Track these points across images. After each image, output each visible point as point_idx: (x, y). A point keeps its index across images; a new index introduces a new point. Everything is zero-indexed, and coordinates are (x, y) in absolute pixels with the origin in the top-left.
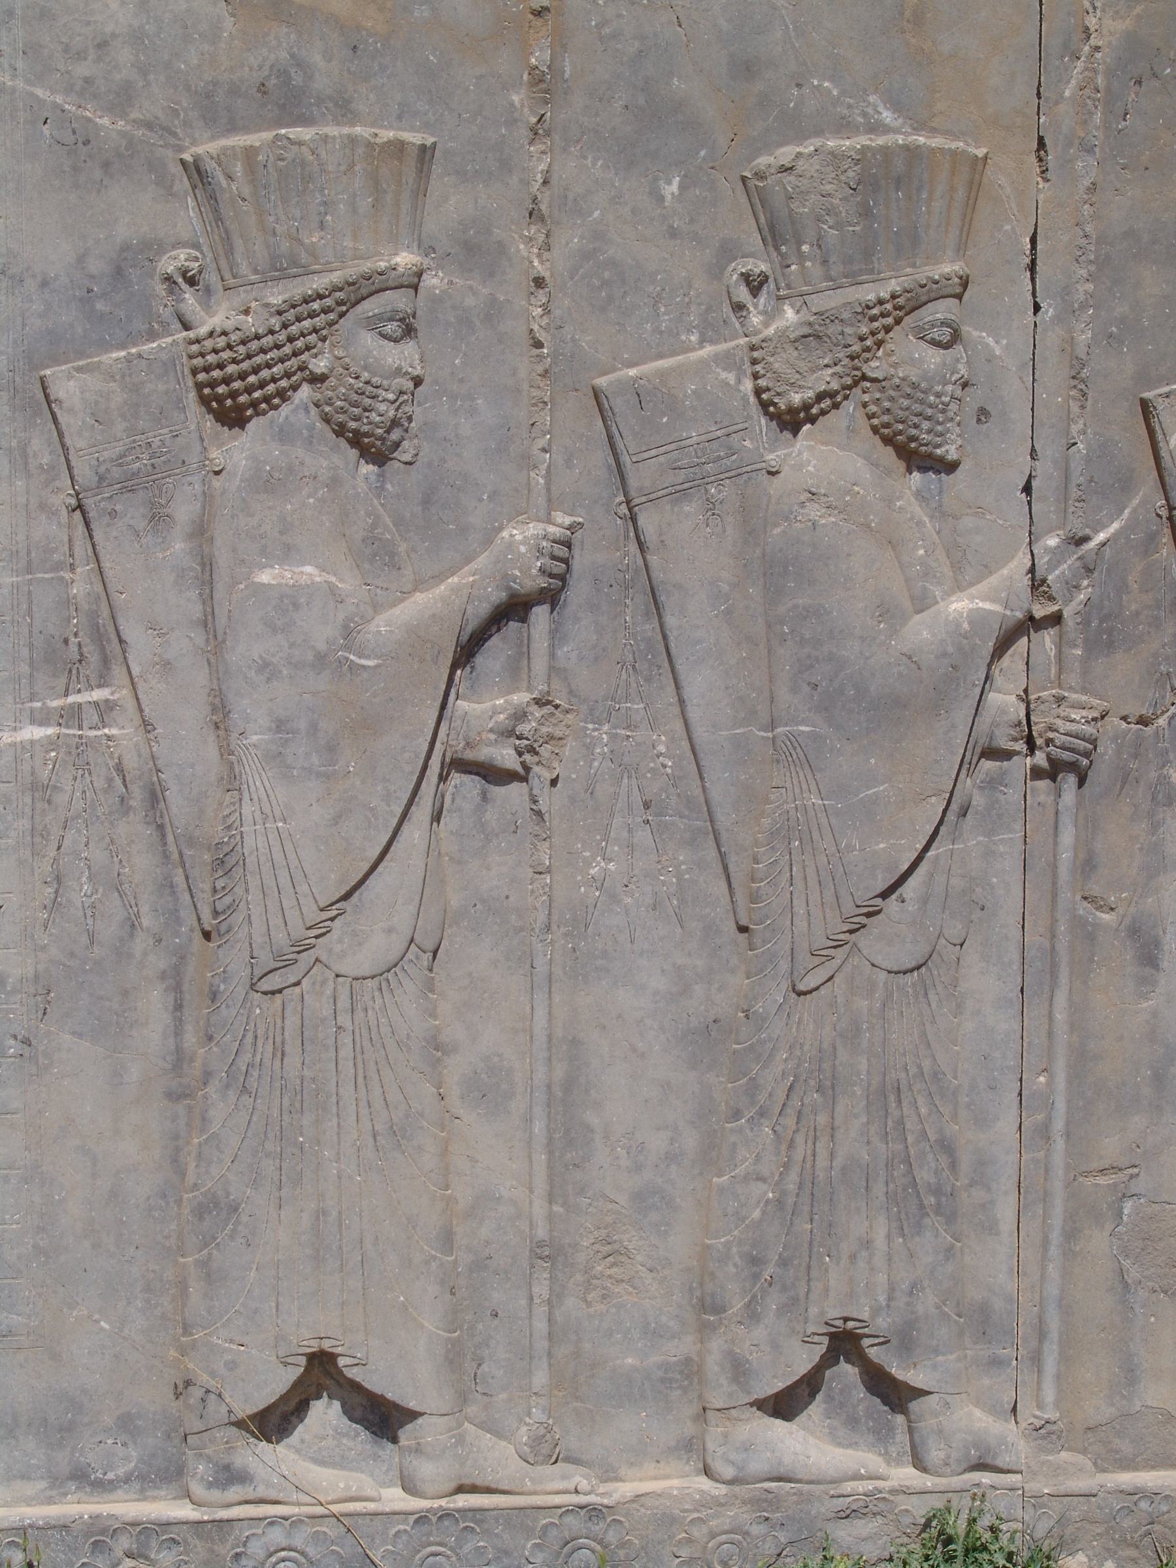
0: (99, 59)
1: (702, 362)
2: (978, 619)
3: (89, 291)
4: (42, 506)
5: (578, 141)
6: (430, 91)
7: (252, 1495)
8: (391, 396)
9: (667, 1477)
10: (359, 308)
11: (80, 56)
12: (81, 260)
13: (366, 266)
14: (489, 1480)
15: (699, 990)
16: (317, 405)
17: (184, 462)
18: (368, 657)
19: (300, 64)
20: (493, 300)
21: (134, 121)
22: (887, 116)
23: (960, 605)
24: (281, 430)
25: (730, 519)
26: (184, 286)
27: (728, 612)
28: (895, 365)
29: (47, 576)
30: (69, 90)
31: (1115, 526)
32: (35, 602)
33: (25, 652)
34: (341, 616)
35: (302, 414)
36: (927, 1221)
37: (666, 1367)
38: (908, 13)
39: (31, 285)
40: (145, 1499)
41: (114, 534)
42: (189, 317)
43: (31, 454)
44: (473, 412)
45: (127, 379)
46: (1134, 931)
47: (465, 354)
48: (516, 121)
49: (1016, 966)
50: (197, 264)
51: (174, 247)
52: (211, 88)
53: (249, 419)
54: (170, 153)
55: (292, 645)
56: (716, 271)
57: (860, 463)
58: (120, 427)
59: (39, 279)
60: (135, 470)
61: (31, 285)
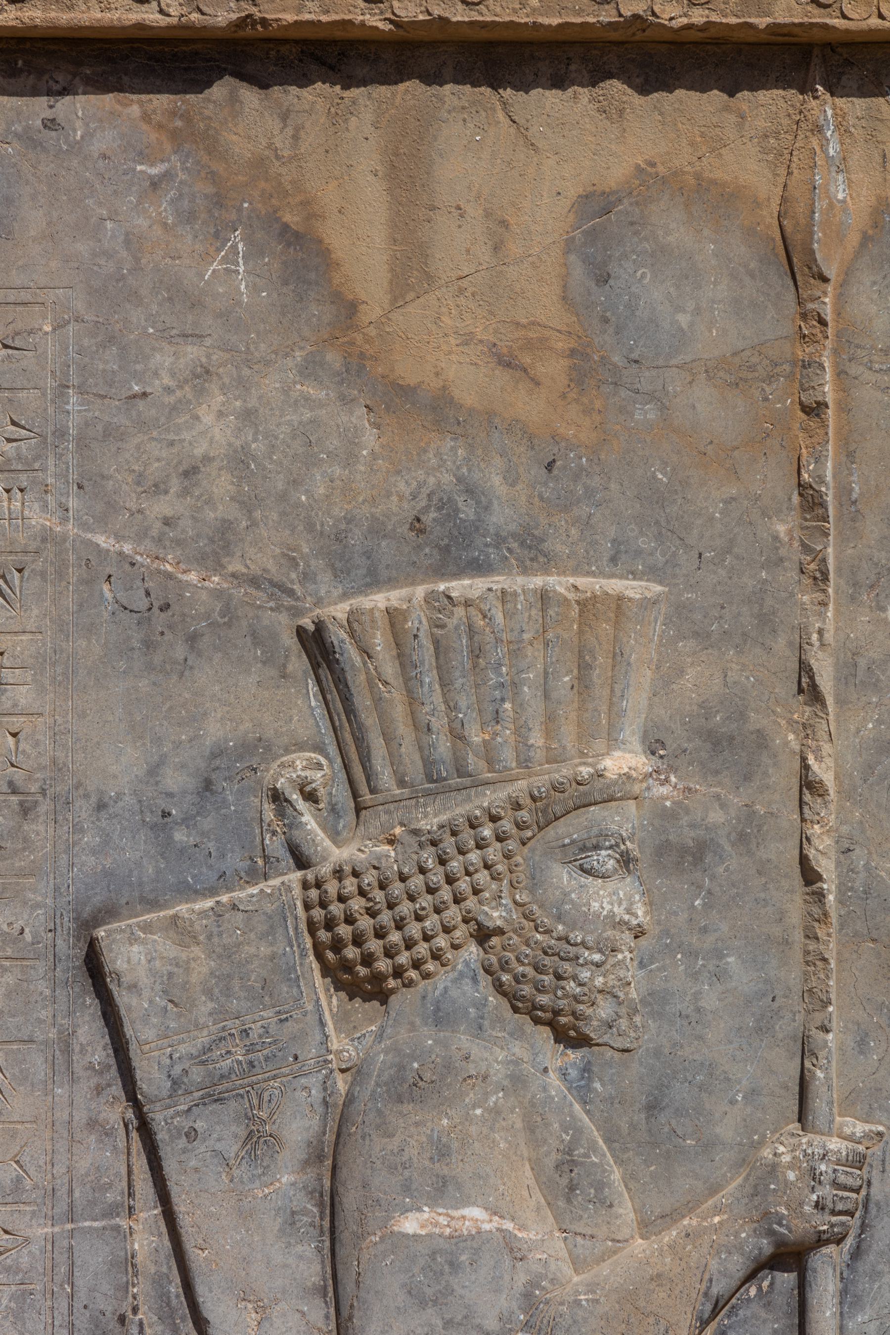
0: (185, 492)
3: (166, 814)
4: (92, 1124)
5: (872, 587)
6: (657, 523)
8: (597, 957)
10: (551, 832)
11: (158, 489)
12: (154, 771)
13: (563, 773)
16: (488, 971)
17: (296, 1058)
19: (470, 491)
21: (233, 575)
24: (438, 1009)
26: (301, 805)
29: (96, 1224)
30: (141, 535)
32: (78, 1262)
34: (522, 1278)
35: (467, 985)
39: (83, 809)
41: (193, 1163)
42: (307, 850)
43: (77, 1048)
44: (719, 976)
45: (216, 940)
47: (709, 892)
48: (781, 560)
50: (319, 774)
51: (287, 751)
52: (343, 526)
53: (392, 991)
54: (283, 618)
58: (205, 1006)
59: (94, 799)
60: (225, 1071)
61: (83, 809)
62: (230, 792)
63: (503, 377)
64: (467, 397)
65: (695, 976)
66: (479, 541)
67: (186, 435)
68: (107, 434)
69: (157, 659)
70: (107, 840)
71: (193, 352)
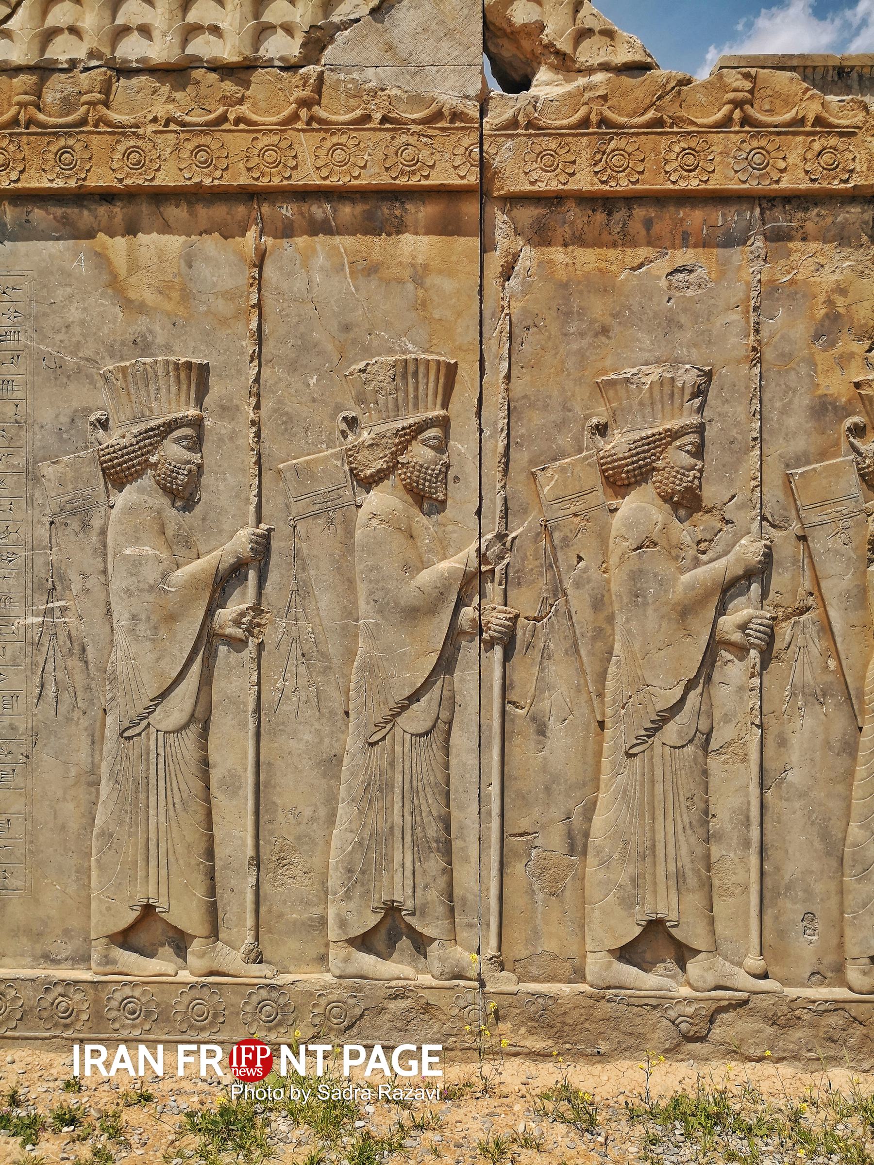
0: (67, 332)
1: (326, 457)
2: (452, 572)
3: (60, 429)
7: (117, 970)
9: (313, 973)
11: (59, 331)
12: (57, 416)
14: (224, 969)
15: (327, 741)
18: (172, 587)
20: (234, 431)
22: (410, 347)
23: (444, 566)
25: (339, 526)
27: (338, 568)
28: (412, 457)
31: (521, 529)
33: (30, 585)
34: (161, 568)
36: (432, 855)
37: (311, 919)
38: (419, 302)
40: (74, 969)
44: (225, 480)
46: (534, 719)
49: (476, 733)
55: (139, 582)
56: (333, 418)
57: (397, 501)
58: (70, 487)
62: (79, 422)
63: (160, 298)
64: (149, 303)
65: (217, 480)
66: (153, 348)
67: (67, 315)
68: (43, 315)
69: (58, 383)
70: (43, 437)
71: (68, 289)
